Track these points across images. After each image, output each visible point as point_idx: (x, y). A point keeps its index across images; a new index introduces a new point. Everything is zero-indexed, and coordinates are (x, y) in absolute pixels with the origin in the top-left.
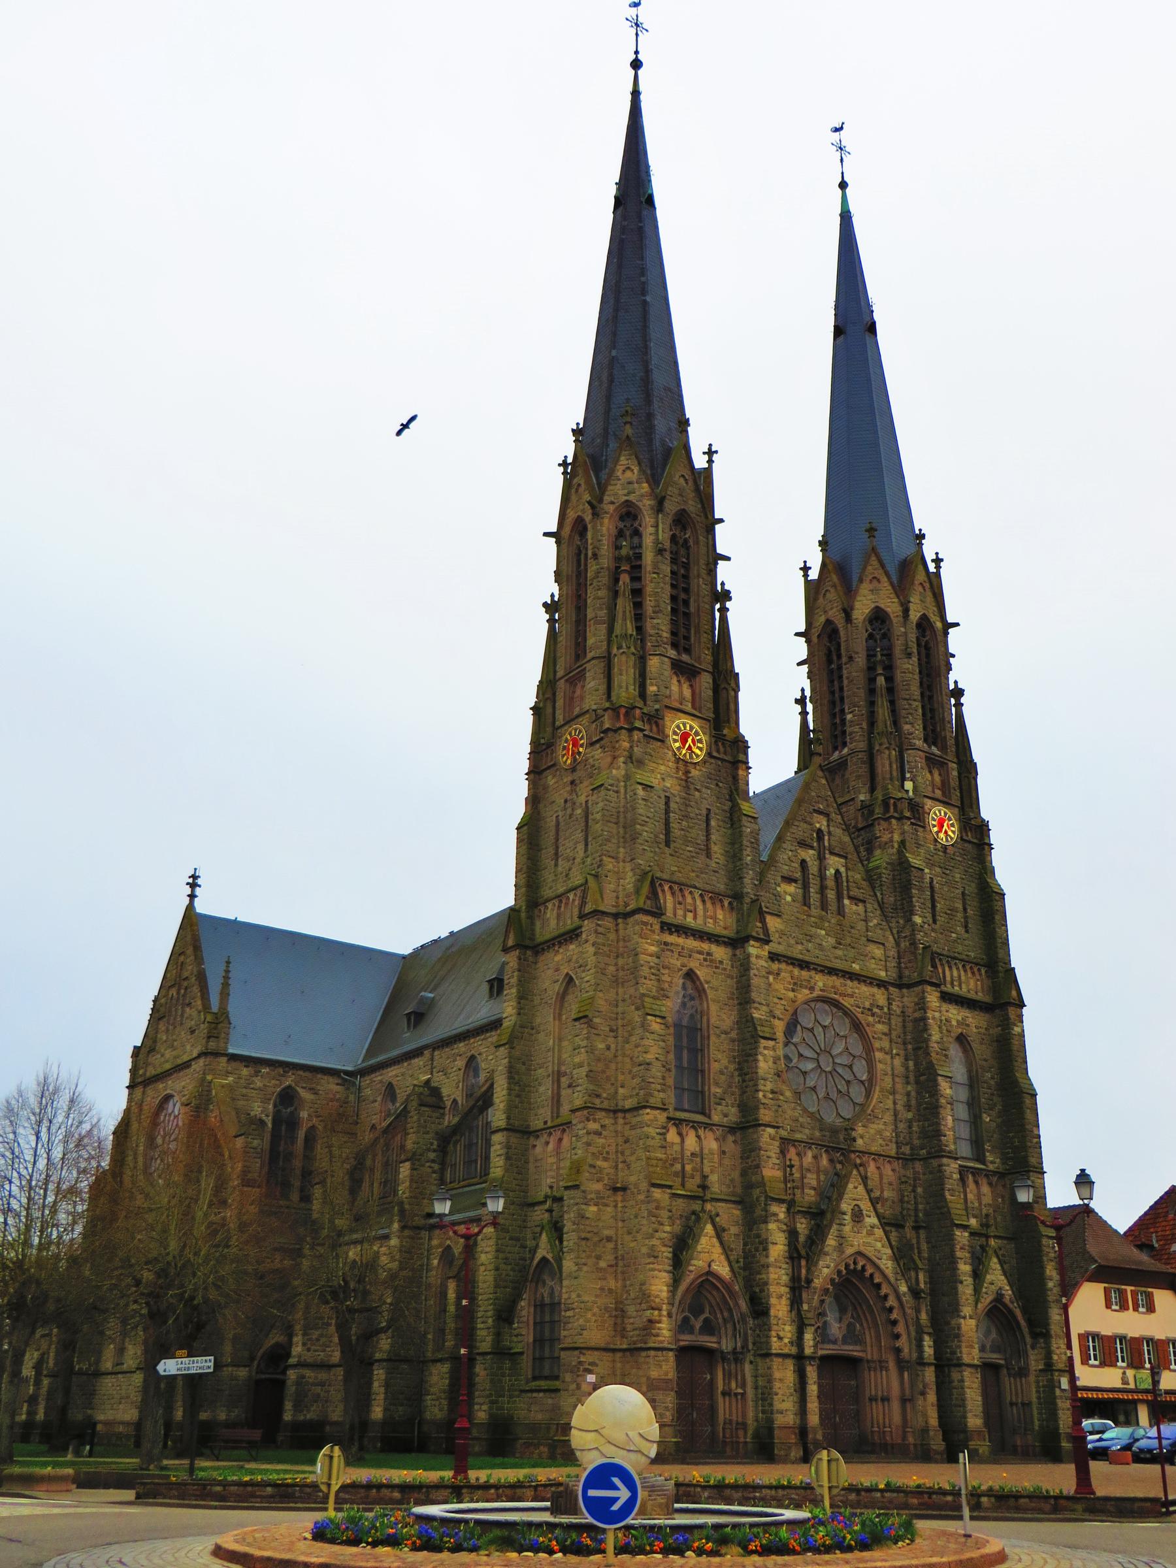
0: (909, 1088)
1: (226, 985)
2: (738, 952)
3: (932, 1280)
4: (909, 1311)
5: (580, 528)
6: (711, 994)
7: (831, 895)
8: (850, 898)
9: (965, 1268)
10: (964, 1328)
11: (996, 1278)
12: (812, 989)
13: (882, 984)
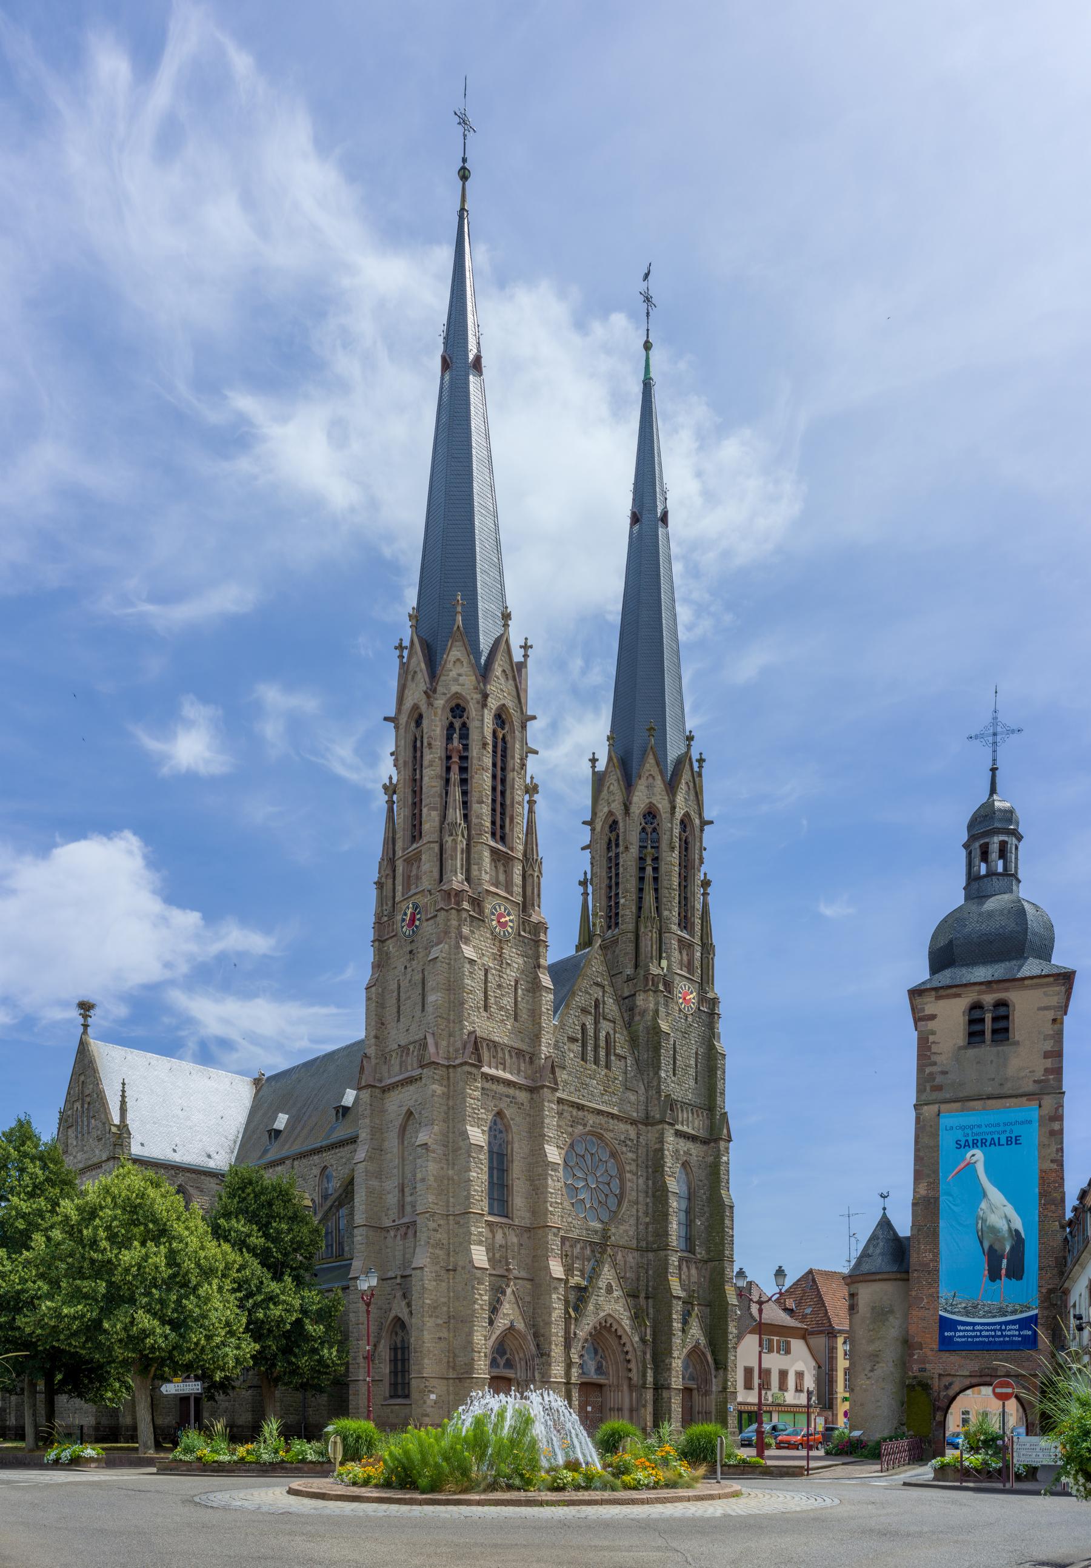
0: (648, 1200)
1: (123, 1103)
2: (534, 1096)
3: (654, 1334)
4: (639, 1353)
5: (416, 716)
6: (514, 1129)
7: (602, 1053)
8: (615, 1055)
9: (677, 1325)
10: (674, 1365)
11: (696, 1331)
12: (585, 1125)
13: (634, 1122)
